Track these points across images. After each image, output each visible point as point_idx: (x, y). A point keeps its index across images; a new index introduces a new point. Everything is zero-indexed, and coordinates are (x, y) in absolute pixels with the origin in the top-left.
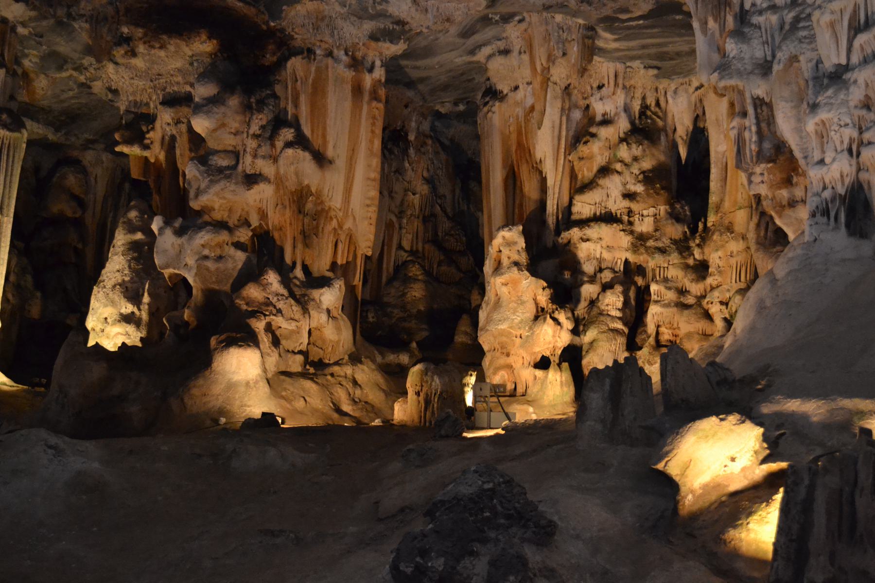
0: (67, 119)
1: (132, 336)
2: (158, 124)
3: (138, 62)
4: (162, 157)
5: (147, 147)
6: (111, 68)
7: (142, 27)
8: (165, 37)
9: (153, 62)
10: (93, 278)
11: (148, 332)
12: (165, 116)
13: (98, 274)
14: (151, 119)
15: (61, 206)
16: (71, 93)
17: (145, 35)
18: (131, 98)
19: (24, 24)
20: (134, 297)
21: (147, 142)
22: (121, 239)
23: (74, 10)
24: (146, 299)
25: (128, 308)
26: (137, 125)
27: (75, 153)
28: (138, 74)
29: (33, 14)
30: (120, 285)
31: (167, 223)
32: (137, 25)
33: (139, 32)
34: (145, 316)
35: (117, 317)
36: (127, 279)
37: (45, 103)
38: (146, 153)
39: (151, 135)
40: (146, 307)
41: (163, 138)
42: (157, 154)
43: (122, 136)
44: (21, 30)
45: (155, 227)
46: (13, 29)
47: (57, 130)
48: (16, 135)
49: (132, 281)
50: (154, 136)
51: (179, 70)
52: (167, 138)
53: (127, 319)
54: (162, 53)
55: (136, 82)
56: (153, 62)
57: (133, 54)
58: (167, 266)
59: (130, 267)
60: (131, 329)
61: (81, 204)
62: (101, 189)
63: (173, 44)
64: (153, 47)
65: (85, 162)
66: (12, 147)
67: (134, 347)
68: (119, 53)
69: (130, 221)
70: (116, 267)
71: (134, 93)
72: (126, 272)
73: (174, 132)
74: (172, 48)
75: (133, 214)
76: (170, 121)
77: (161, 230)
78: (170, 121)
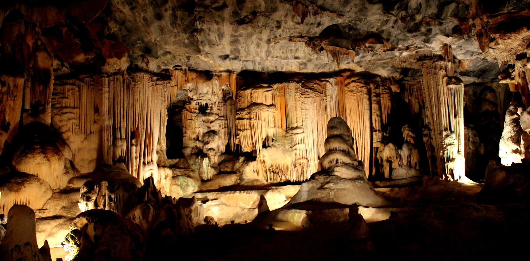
0: (482, 73)
1: (518, 159)
2: (516, 68)
3: (501, 46)
4: (520, 81)
5: (513, 79)
6: (491, 51)
7: (498, 33)
8: (508, 34)
9: (507, 45)
10: (499, 136)
11: (525, 156)
12: (518, 65)
13: (501, 134)
14: (512, 66)
15: (486, 107)
16: (480, 63)
17: (500, 36)
18: (503, 60)
19: (453, 44)
20: (517, 142)
21: (512, 76)
22: (508, 119)
23: (470, 35)
24: (522, 142)
25: (515, 147)
26: (507, 71)
27: (489, 85)
28: (504, 51)
29: (456, 39)
30: (510, 138)
31: (524, 110)
32: (495, 33)
33: (497, 36)
34: (522, 149)
35: (511, 151)
36: (513, 135)
37: (471, 69)
38: (513, 81)
39: (514, 73)
40: (523, 146)
41: (519, 74)
42: (518, 80)
43: (502, 77)
44: (453, 46)
45: (519, 112)
46: (450, 47)
47: (479, 78)
48: (459, 86)
49: (515, 135)
50: (515, 73)
51: (519, 45)
52: (521, 73)
53: (516, 151)
54: (509, 41)
55: (502, 54)
56: (507, 45)
57: (497, 44)
58: (527, 128)
59: (513, 130)
60: (518, 155)
61: (495, 104)
62: (502, 97)
63: (513, 36)
64: (505, 39)
65: (494, 88)
66: (458, 91)
67: (518, 164)
68: (492, 44)
69: (510, 111)
70: (508, 130)
71: (504, 58)
72: (512, 132)
73: (524, 70)
74: (513, 38)
75: (511, 108)
76: (521, 66)
77: (521, 113)
78: (521, 66)
